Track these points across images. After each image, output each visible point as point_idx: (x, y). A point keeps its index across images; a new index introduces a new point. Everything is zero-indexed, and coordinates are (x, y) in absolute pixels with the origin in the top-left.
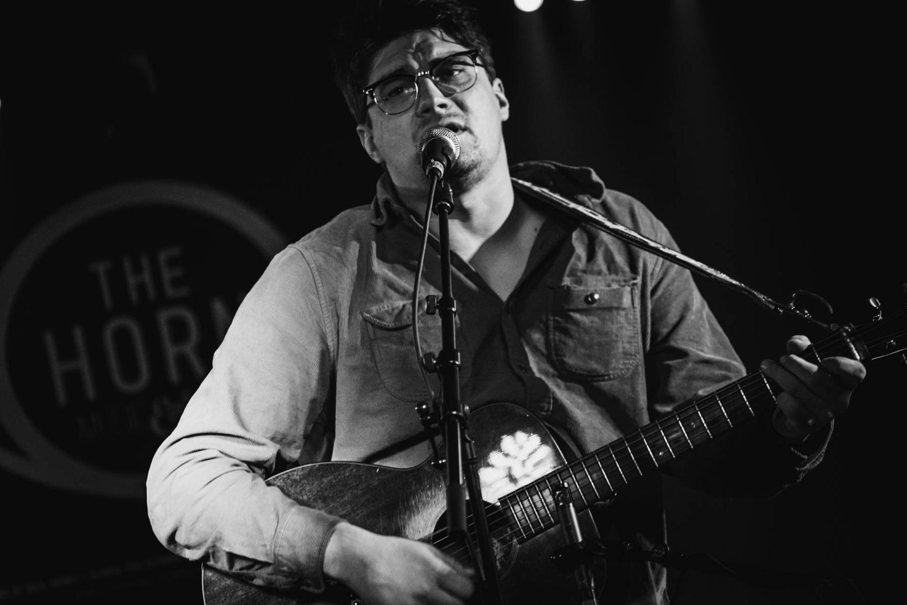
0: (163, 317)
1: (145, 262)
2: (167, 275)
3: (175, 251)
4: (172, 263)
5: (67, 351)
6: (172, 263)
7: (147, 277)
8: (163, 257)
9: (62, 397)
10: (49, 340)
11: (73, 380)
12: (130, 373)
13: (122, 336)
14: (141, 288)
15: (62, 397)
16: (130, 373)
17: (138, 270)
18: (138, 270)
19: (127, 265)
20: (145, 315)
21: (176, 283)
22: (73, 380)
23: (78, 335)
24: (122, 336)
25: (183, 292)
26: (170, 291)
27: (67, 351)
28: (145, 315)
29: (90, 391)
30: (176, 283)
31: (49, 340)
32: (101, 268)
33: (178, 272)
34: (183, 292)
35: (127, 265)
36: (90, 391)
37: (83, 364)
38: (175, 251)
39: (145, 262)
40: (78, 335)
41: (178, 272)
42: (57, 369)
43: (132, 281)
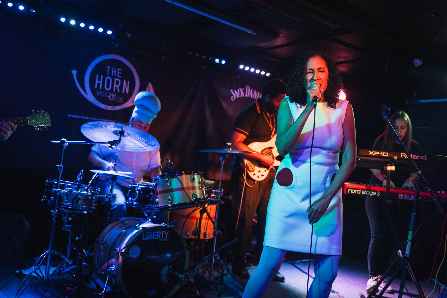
0: (116, 79)
1: (116, 69)
2: (118, 73)
3: (121, 70)
4: (120, 71)
5: (99, 79)
6: (120, 71)
7: (115, 72)
8: (119, 69)
9: (96, 87)
10: (97, 76)
11: (99, 84)
12: (108, 87)
13: (108, 80)
14: (114, 73)
15: (96, 87)
16: (108, 87)
17: (114, 70)
18: (114, 70)
19: (113, 68)
20: (113, 78)
21: (119, 75)
22: (99, 84)
23: (102, 77)
24: (108, 80)
25: (120, 77)
26: (118, 76)
27: (99, 79)
28: (113, 78)
29: (101, 88)
30: (119, 75)
31: (97, 76)
33: (120, 73)
34: (120, 77)
35: (113, 68)
36: (101, 88)
37: (101, 82)
38: (121, 70)
39: (116, 69)
40: (102, 77)
41: (120, 73)
42: (97, 81)
43: (113, 72)
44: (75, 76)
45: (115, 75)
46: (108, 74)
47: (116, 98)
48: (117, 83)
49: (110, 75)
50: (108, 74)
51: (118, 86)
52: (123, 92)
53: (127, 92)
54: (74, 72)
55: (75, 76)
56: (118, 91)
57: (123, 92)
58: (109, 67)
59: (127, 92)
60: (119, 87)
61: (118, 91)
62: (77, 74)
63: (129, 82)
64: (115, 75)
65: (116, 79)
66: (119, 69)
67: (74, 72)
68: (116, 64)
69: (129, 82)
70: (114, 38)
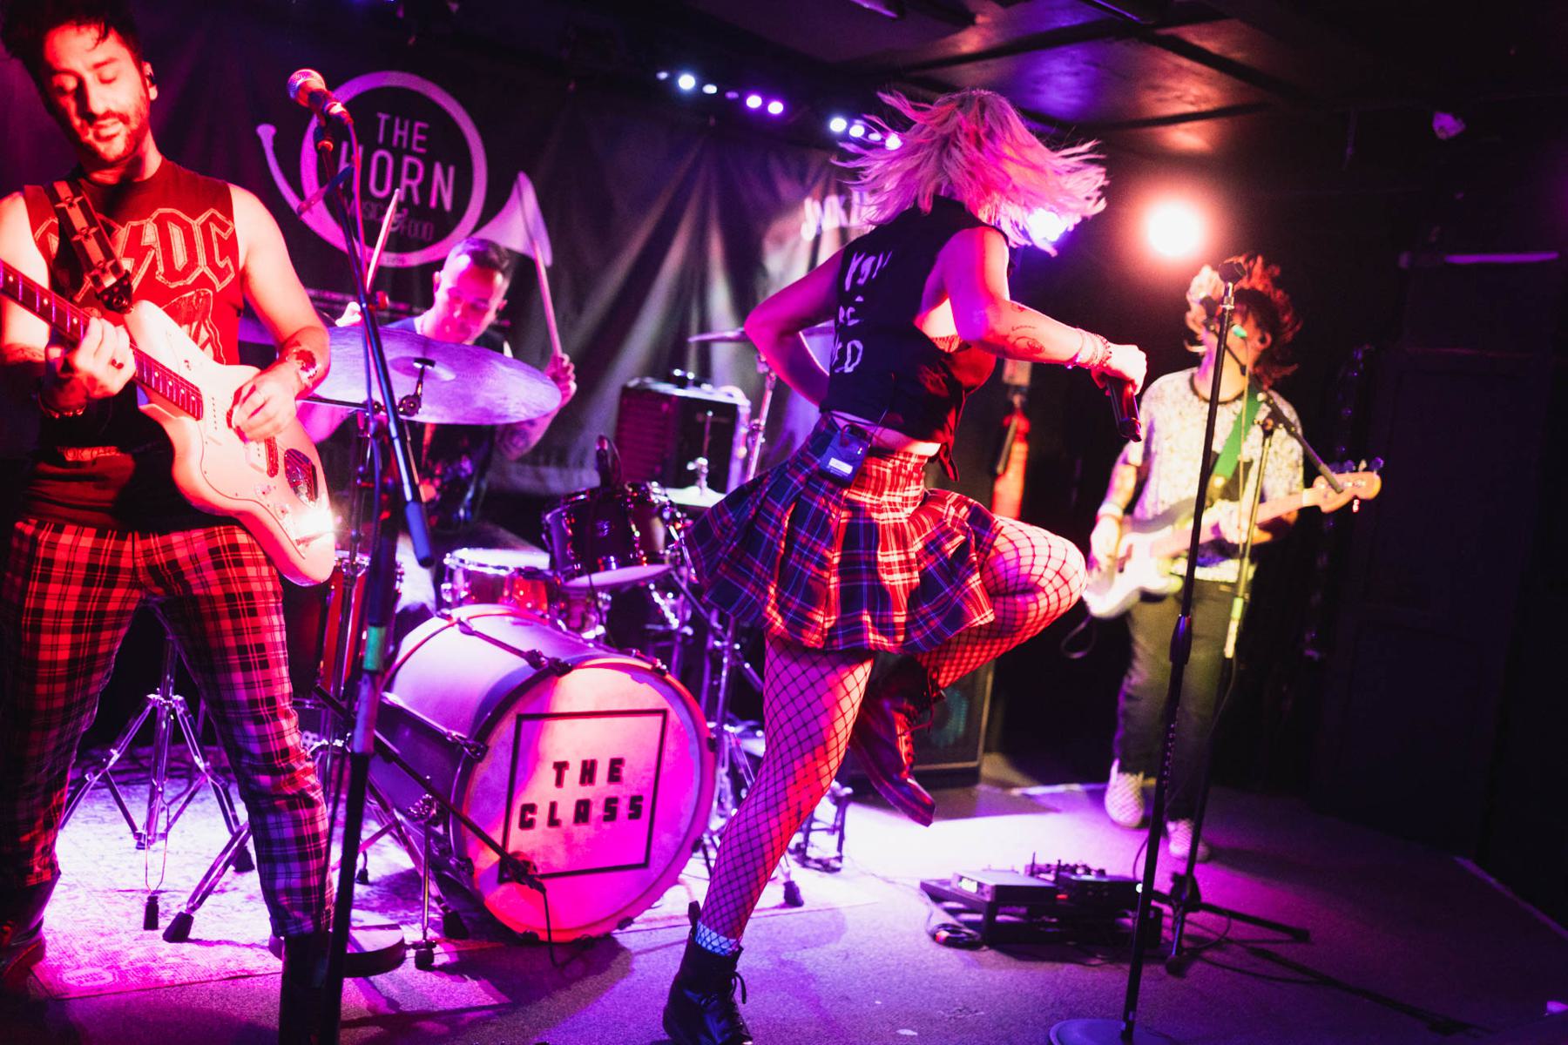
0: (407, 160)
1: (407, 124)
2: (416, 137)
3: (425, 125)
6: (421, 131)
7: (405, 133)
8: (417, 125)
13: (382, 161)
14: (400, 137)
17: (401, 128)
19: (397, 121)
20: (398, 154)
21: (420, 144)
24: (382, 161)
25: (422, 150)
26: (415, 148)
30: (420, 144)
32: (383, 117)
33: (423, 138)
34: (422, 150)
35: (397, 121)
38: (425, 125)
39: (407, 124)
41: (423, 138)
43: (397, 132)
44: (268, 145)
45: (404, 145)
46: (381, 139)
47: (406, 223)
48: (412, 174)
49: (387, 145)
50: (381, 139)
51: (414, 184)
52: (433, 204)
53: (448, 205)
54: (266, 132)
55: (268, 145)
56: (416, 200)
57: (433, 204)
58: (383, 117)
59: (448, 205)
60: (419, 187)
61: (416, 200)
62: (276, 139)
63: (451, 170)
64: (404, 145)
65: (407, 160)
66: (417, 125)
67: (266, 132)
68: (406, 104)
69: (451, 170)
70: (401, 14)
